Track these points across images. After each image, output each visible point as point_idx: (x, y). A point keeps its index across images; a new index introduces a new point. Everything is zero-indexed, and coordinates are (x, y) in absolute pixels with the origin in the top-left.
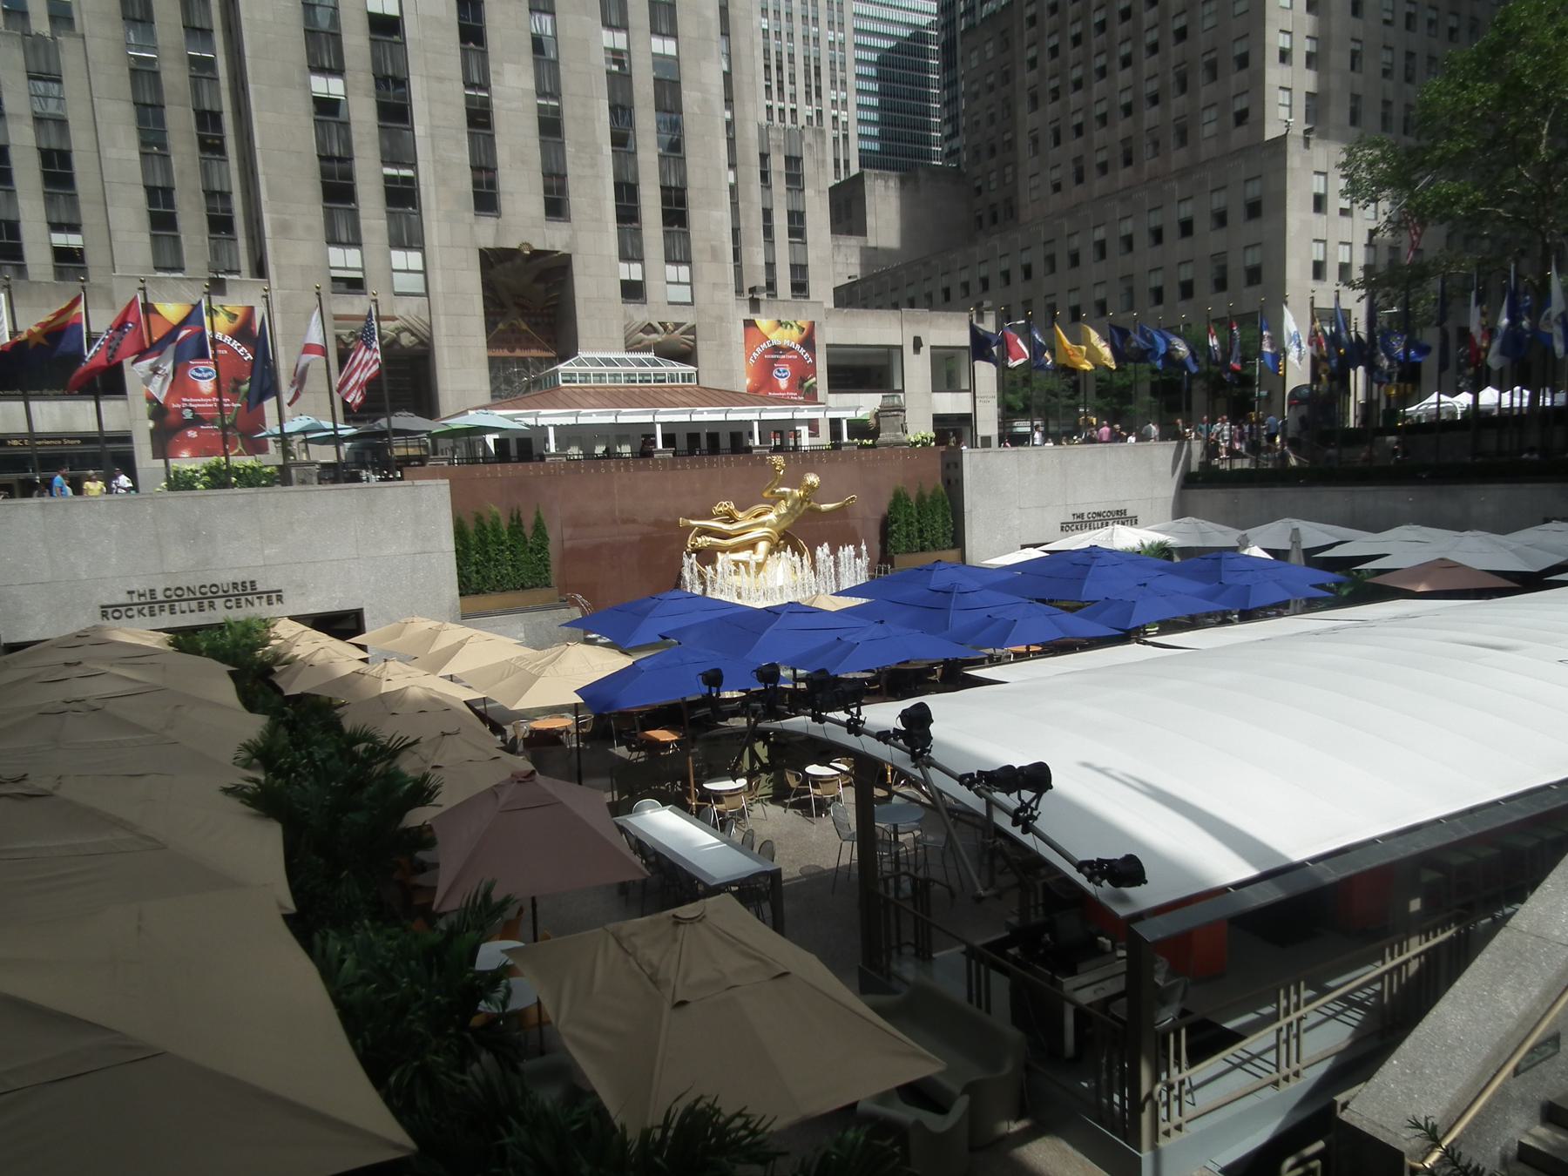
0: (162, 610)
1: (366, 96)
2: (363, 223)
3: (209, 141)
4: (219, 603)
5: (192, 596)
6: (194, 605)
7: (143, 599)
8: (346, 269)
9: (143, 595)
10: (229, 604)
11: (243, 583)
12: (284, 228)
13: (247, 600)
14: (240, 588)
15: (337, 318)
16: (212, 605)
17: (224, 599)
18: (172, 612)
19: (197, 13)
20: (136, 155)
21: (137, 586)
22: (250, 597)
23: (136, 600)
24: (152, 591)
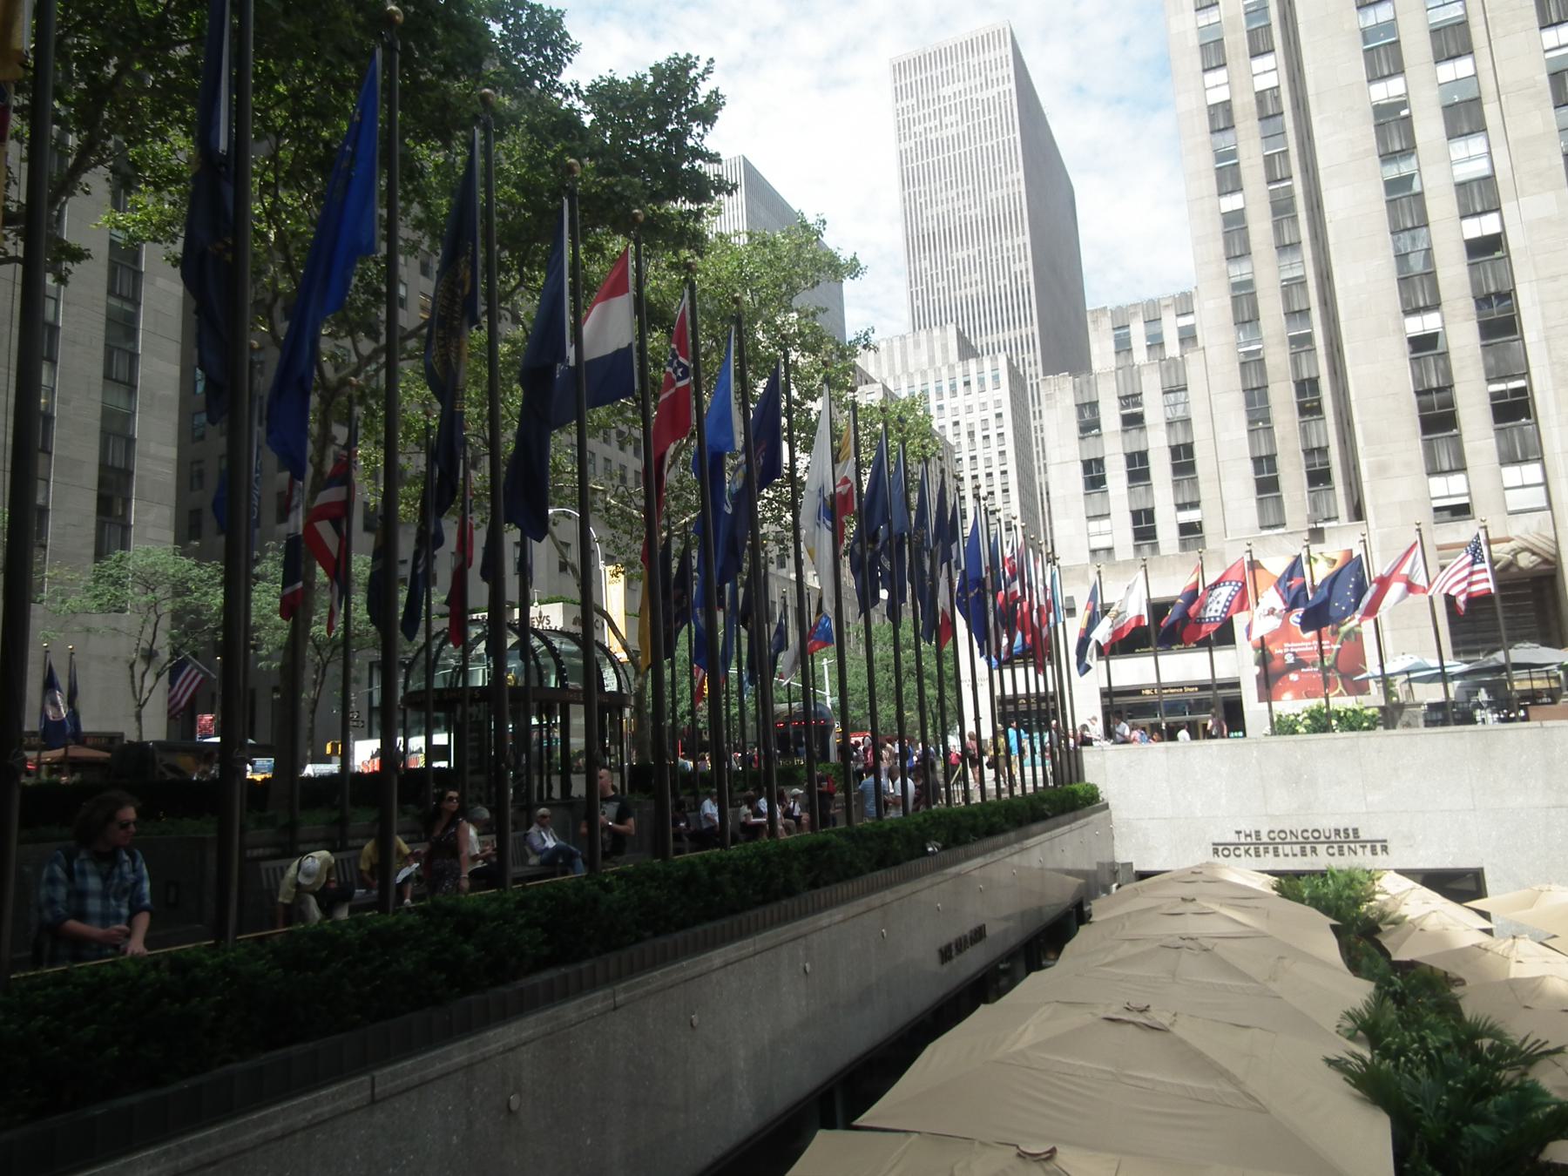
0: (1266, 851)
1: (1466, 320)
2: (1468, 448)
3: (1308, 405)
4: (1321, 848)
5: (1294, 840)
6: (1297, 848)
7: (1249, 839)
8: (1450, 497)
9: (1250, 836)
10: (1331, 851)
11: (1346, 830)
12: (1381, 469)
13: (1349, 848)
14: (1342, 834)
15: (1440, 548)
16: (1314, 850)
17: (1326, 845)
18: (1276, 854)
19: (1296, 299)
20: (1245, 434)
21: (1248, 827)
22: (1352, 846)
23: (1243, 840)
24: (1258, 833)
